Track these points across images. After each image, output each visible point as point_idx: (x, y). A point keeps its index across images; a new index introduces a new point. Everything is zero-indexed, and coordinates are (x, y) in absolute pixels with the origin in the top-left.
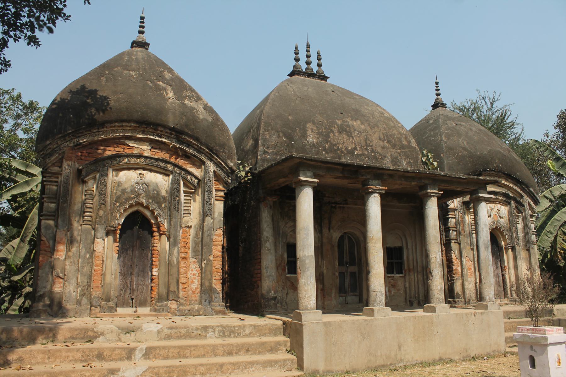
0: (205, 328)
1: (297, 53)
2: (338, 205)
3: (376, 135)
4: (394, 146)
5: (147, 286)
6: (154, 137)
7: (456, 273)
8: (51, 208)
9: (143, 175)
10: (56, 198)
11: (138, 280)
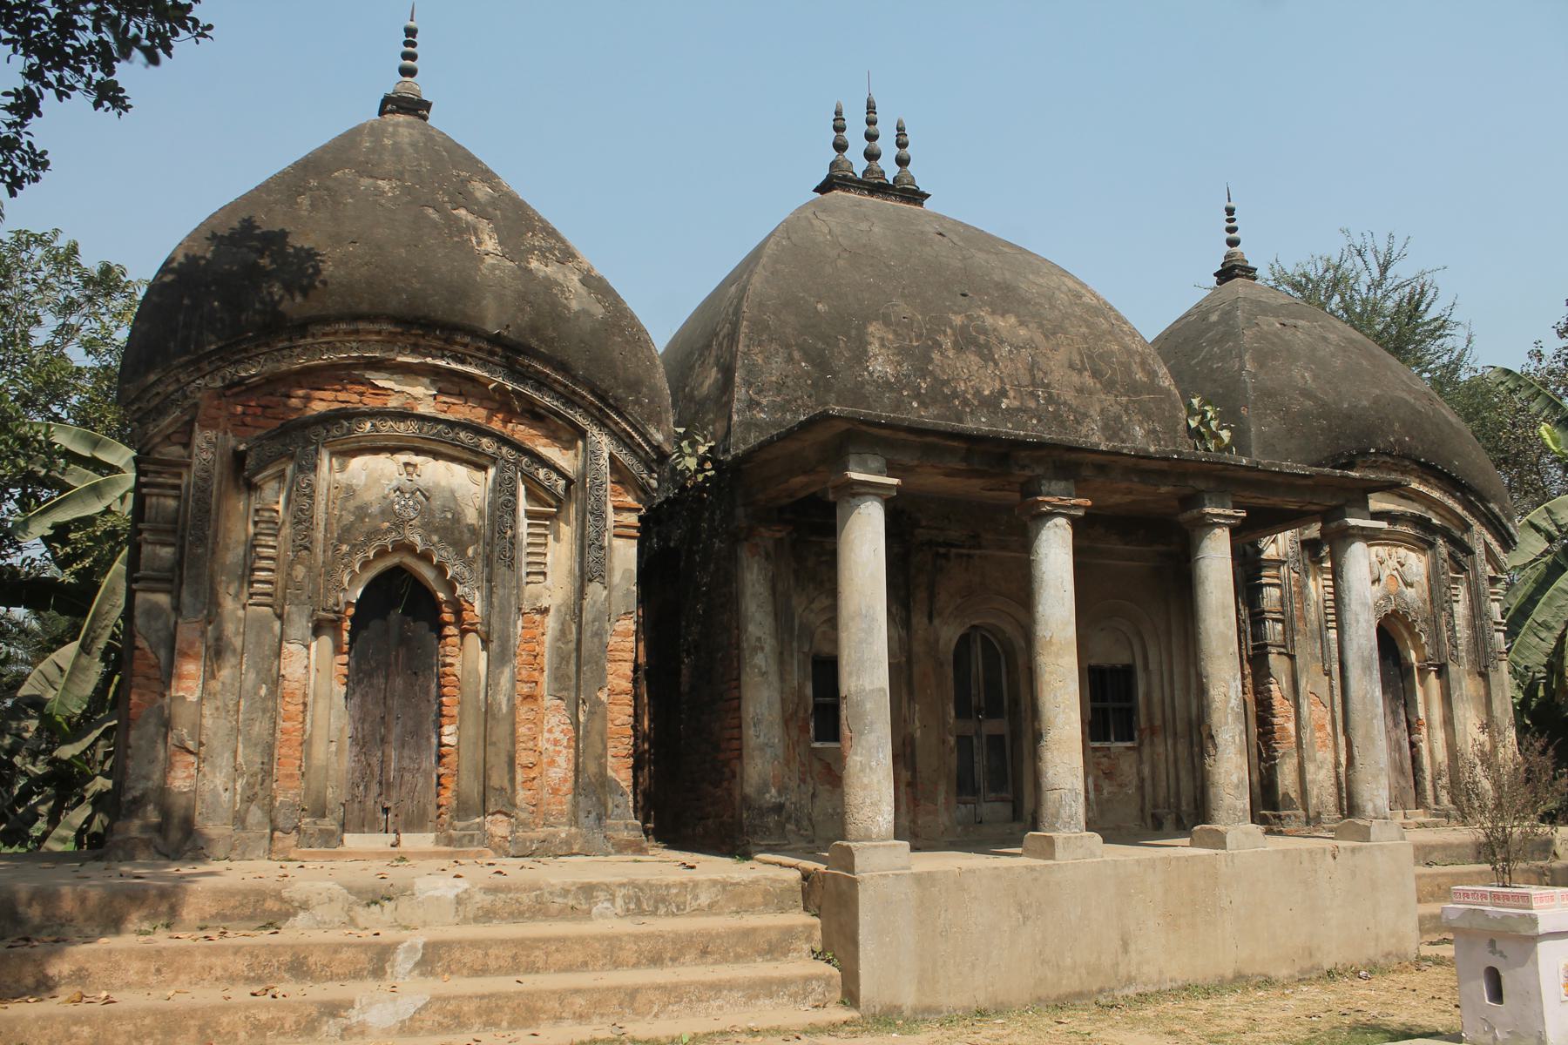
0: (588, 890)
1: (839, 129)
2: (954, 550)
3: (1061, 356)
4: (1109, 386)
5: (428, 775)
6: (443, 363)
8: (161, 558)
9: (415, 466)
10: (174, 532)
11: (400, 758)
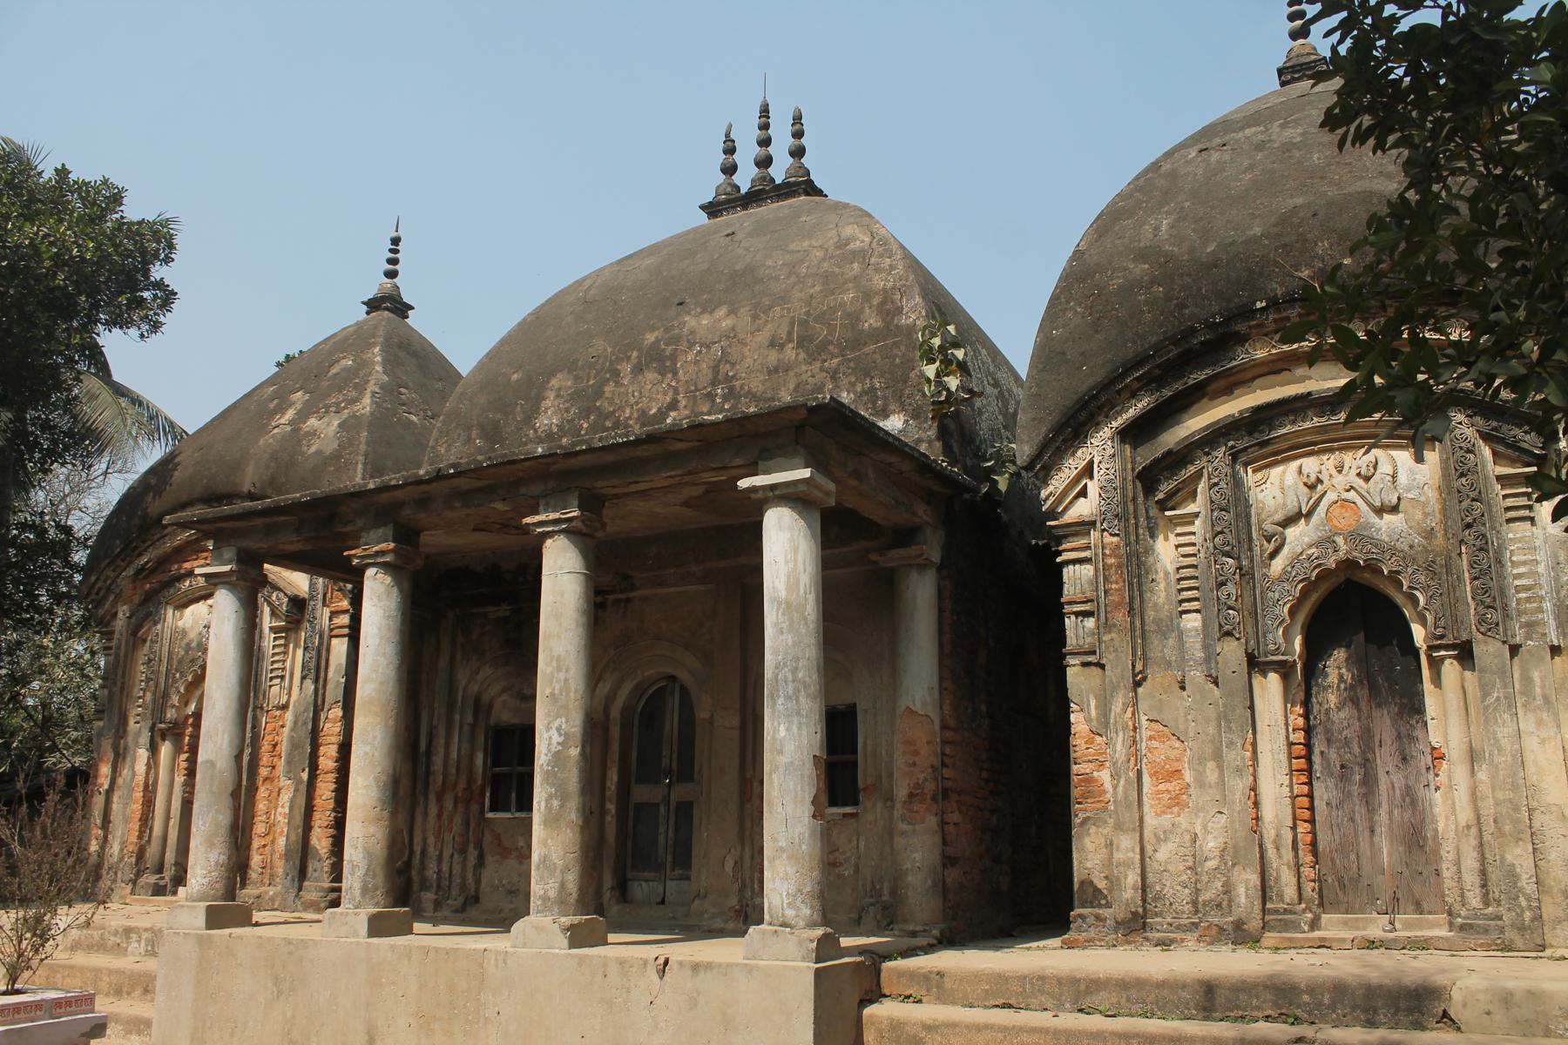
1: (730, 150)
2: (611, 597)
3: (763, 337)
7: (1087, 795)
